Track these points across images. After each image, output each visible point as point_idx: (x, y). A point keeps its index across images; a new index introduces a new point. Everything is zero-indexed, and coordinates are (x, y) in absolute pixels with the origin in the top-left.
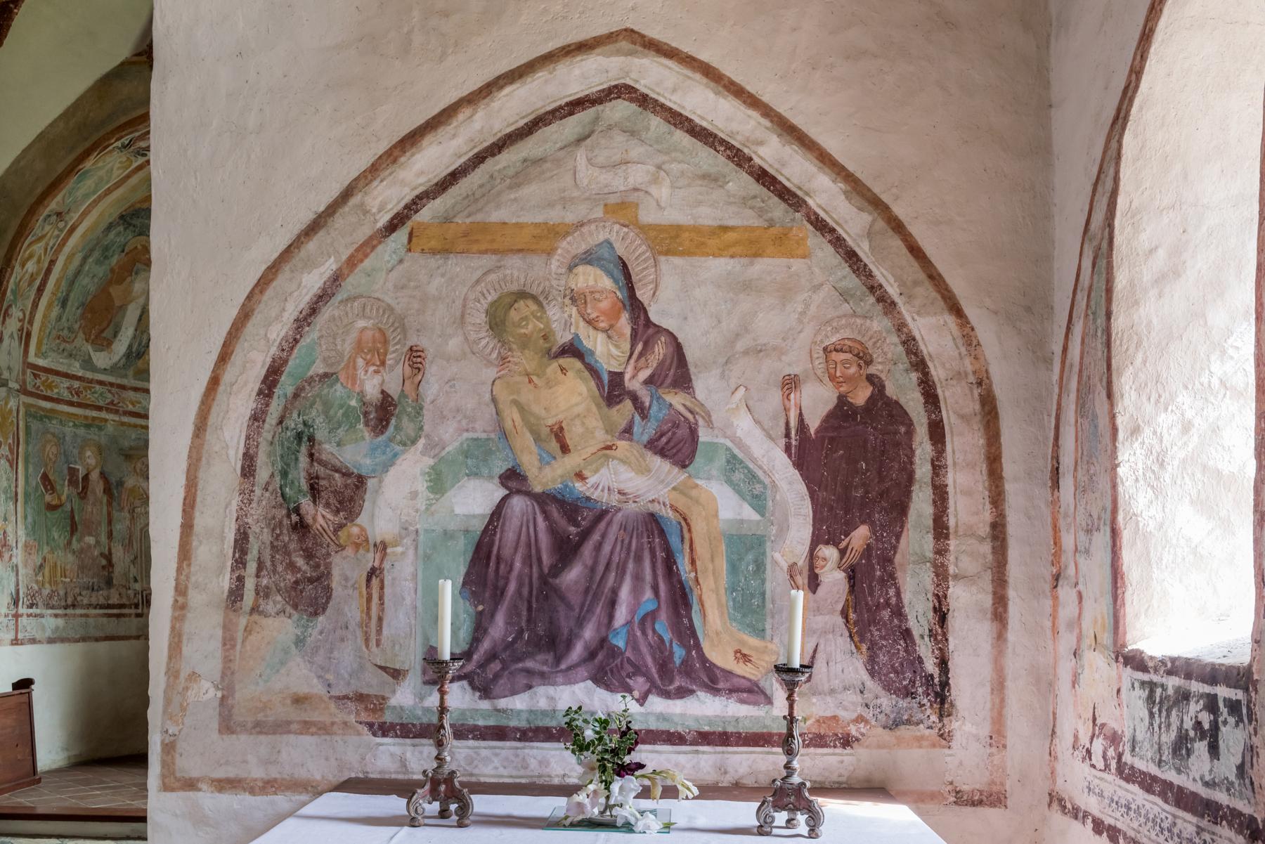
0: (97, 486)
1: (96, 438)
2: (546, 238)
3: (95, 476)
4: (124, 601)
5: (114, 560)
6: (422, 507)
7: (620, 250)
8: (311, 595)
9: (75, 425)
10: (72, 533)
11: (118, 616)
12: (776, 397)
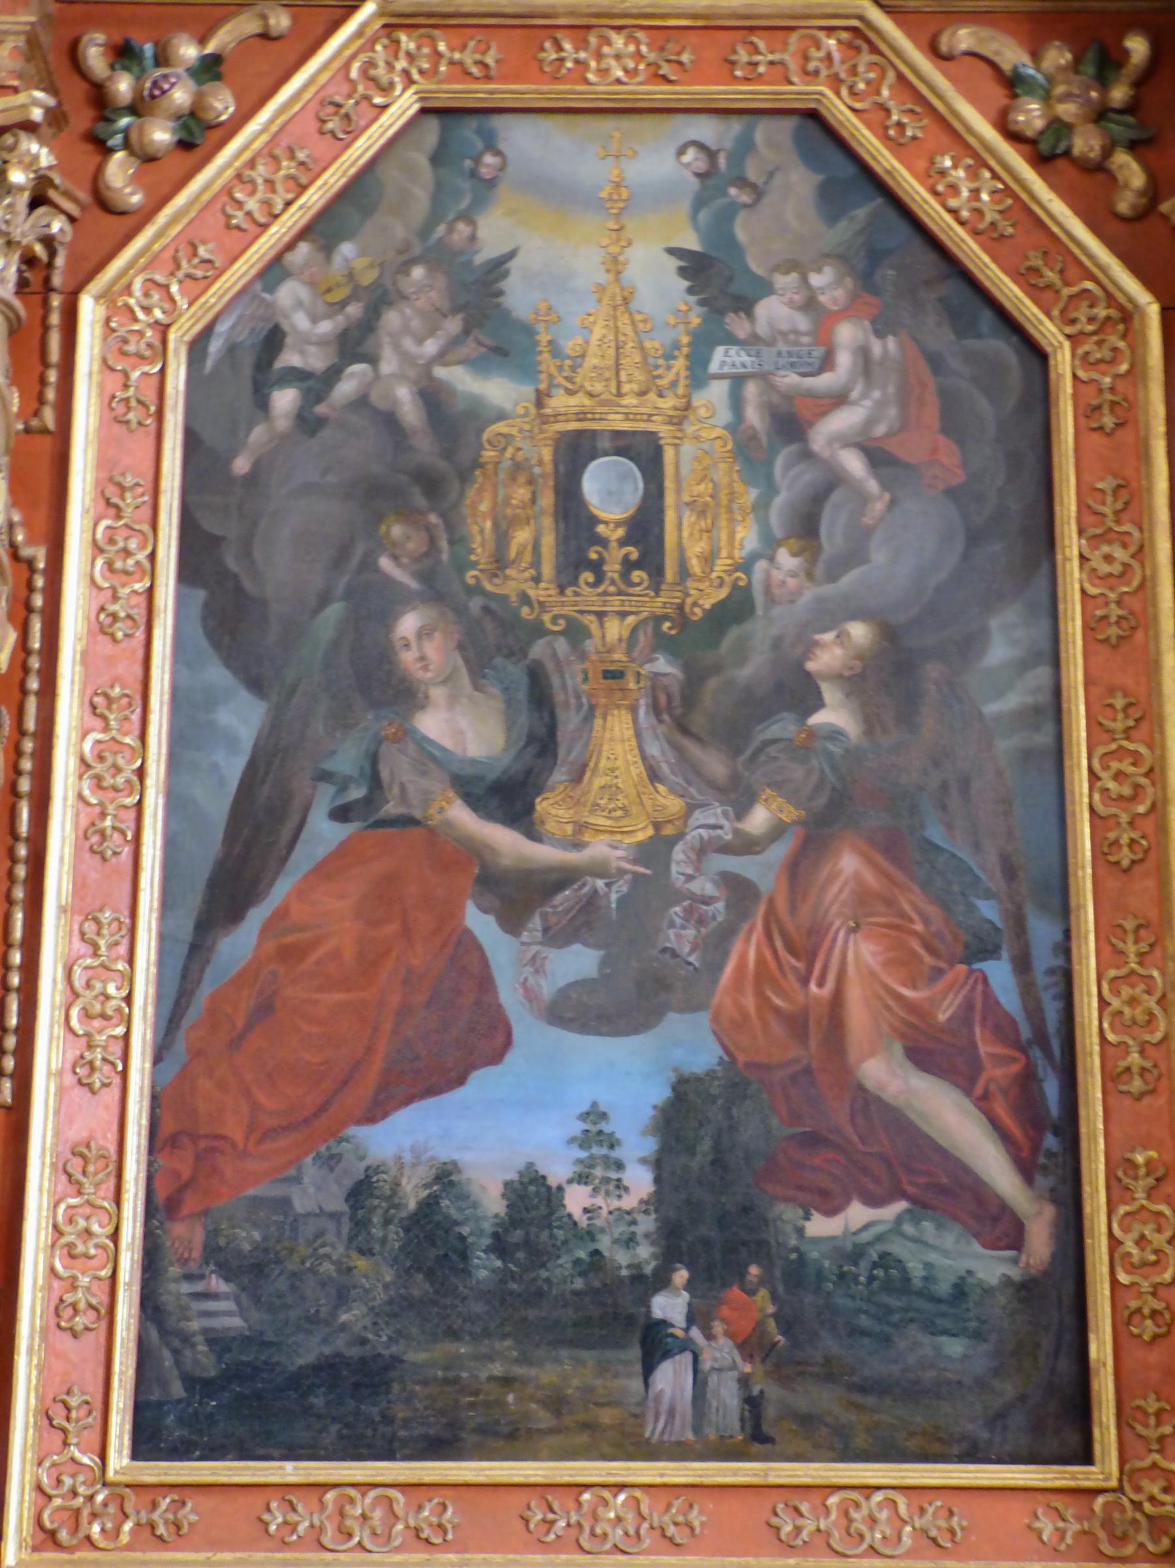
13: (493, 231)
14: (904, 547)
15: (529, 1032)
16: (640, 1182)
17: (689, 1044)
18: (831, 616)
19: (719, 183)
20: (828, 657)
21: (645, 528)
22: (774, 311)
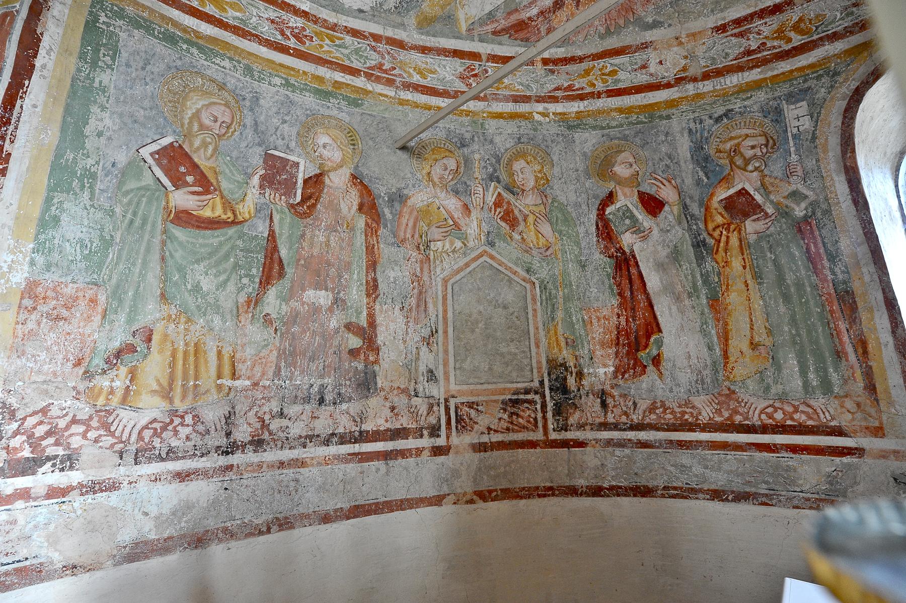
0: (349, 203)
1: (343, 116)
3: (338, 180)
4: (405, 421)
5: (380, 340)
9: (287, 84)
10: (266, 281)
11: (386, 456)
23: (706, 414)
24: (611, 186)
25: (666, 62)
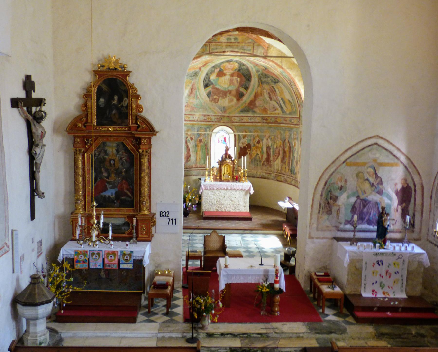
2: (364, 164)
6: (345, 200)
7: (374, 166)
8: (329, 212)
12: (394, 186)
13: (106, 148)
14: (127, 165)
15: (109, 189)
16: (114, 196)
17: (116, 189)
18: (123, 169)
19: (118, 145)
20: (123, 171)
21: (114, 164)
22: (121, 153)
23: (194, 166)
24: (187, 136)
25: (196, 118)
